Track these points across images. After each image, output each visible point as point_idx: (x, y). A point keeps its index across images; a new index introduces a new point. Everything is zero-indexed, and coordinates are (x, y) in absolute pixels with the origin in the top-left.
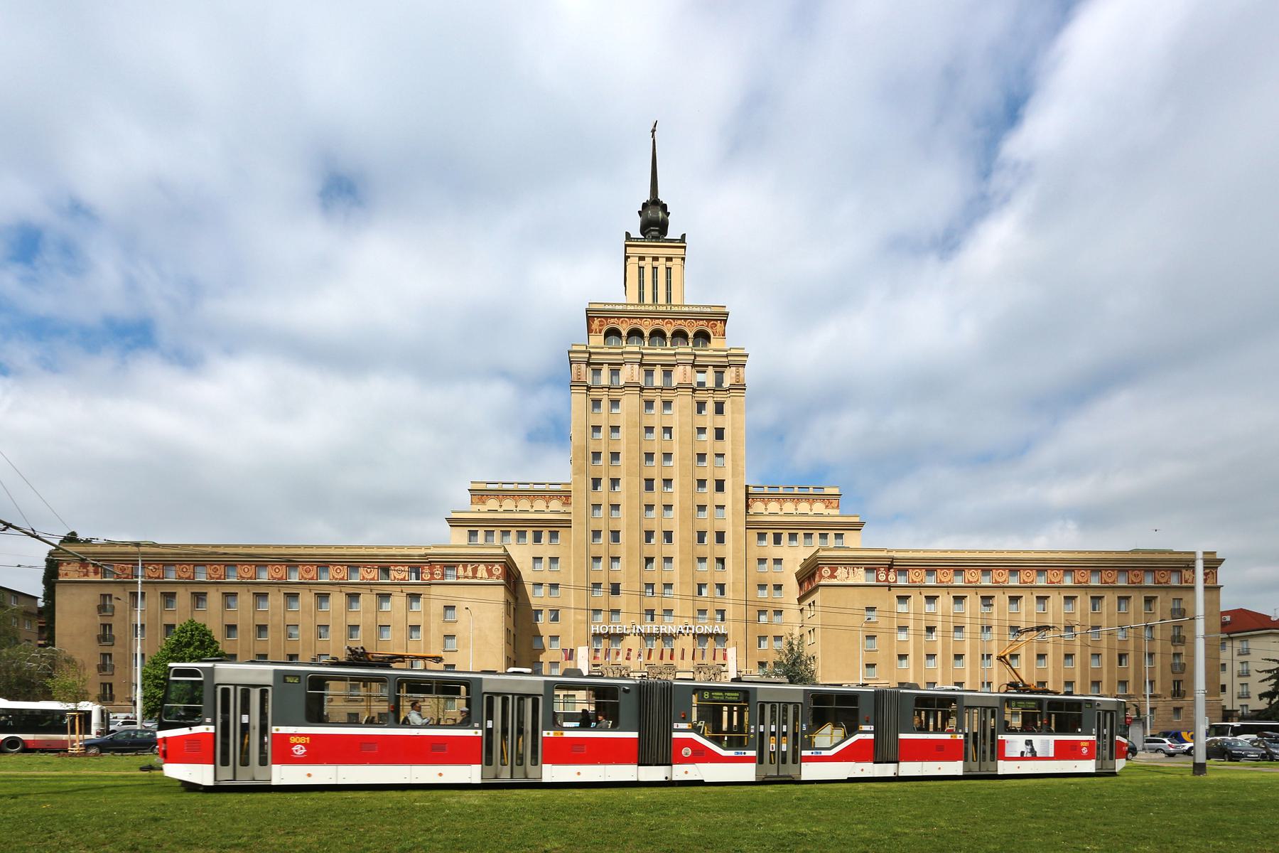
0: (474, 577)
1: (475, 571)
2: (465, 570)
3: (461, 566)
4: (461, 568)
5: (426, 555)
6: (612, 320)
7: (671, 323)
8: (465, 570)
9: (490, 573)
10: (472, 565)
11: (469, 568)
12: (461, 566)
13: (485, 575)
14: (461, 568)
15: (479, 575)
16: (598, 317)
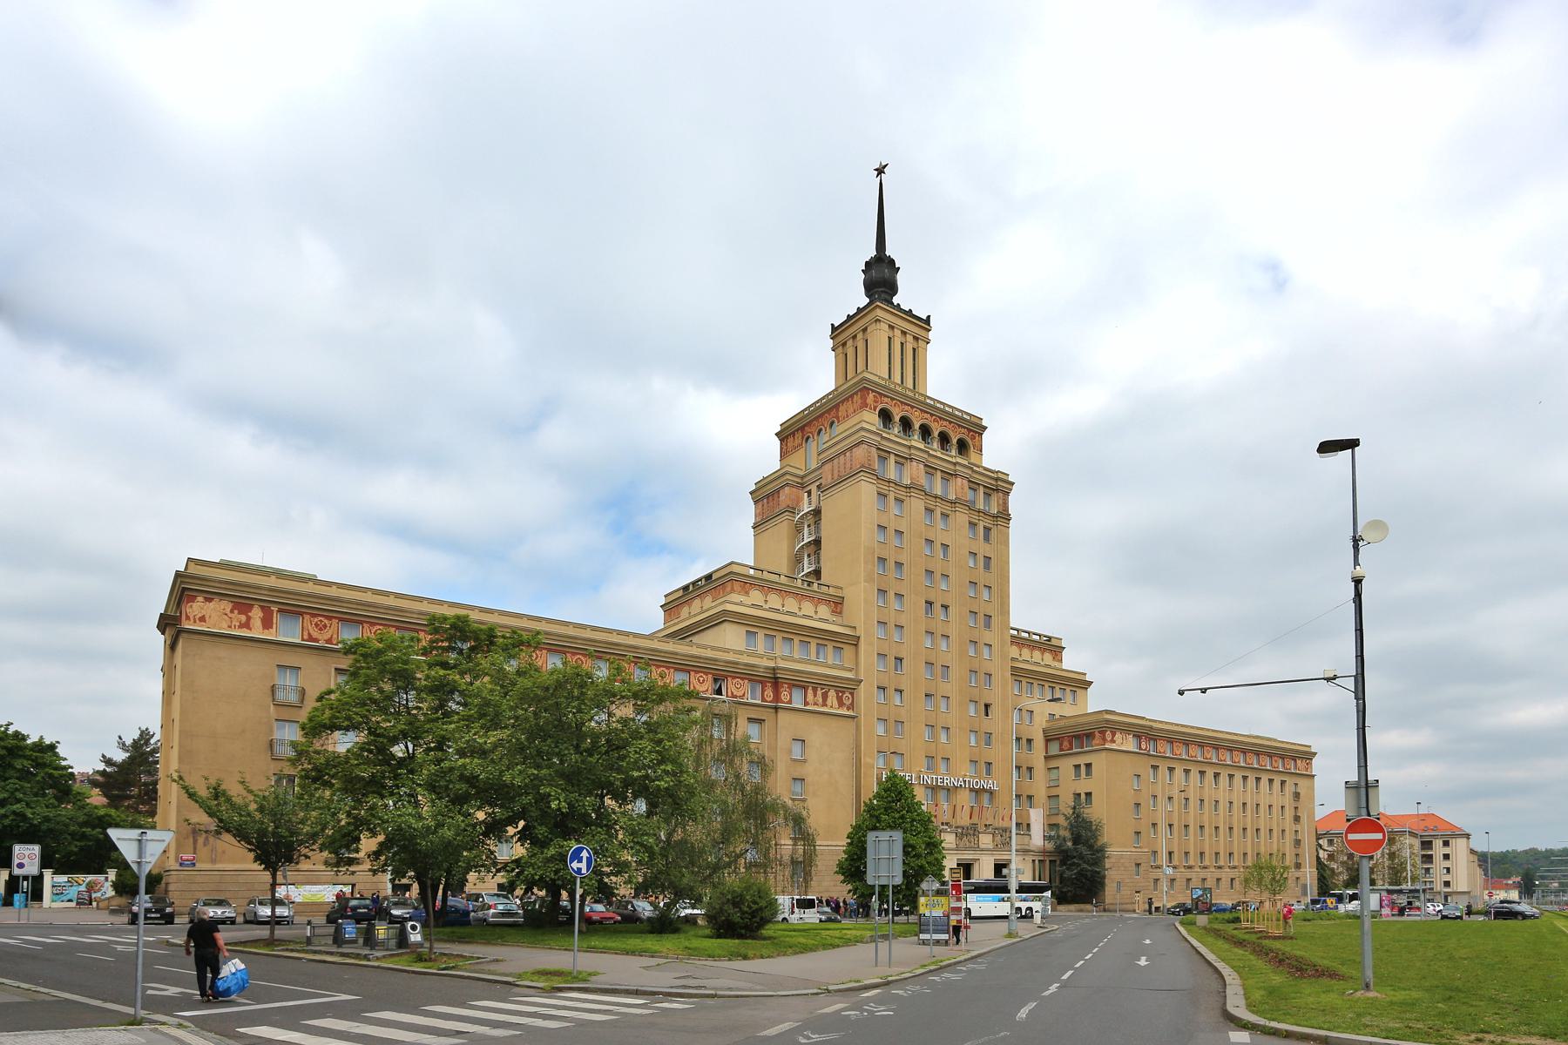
0: (824, 705)
1: (825, 696)
2: (815, 696)
3: (810, 688)
4: (810, 691)
5: (774, 669)
6: (886, 400)
7: (937, 421)
8: (815, 696)
9: (841, 704)
10: (822, 689)
11: (819, 692)
12: (810, 688)
13: (835, 703)
14: (810, 691)
15: (829, 702)
16: (873, 391)
